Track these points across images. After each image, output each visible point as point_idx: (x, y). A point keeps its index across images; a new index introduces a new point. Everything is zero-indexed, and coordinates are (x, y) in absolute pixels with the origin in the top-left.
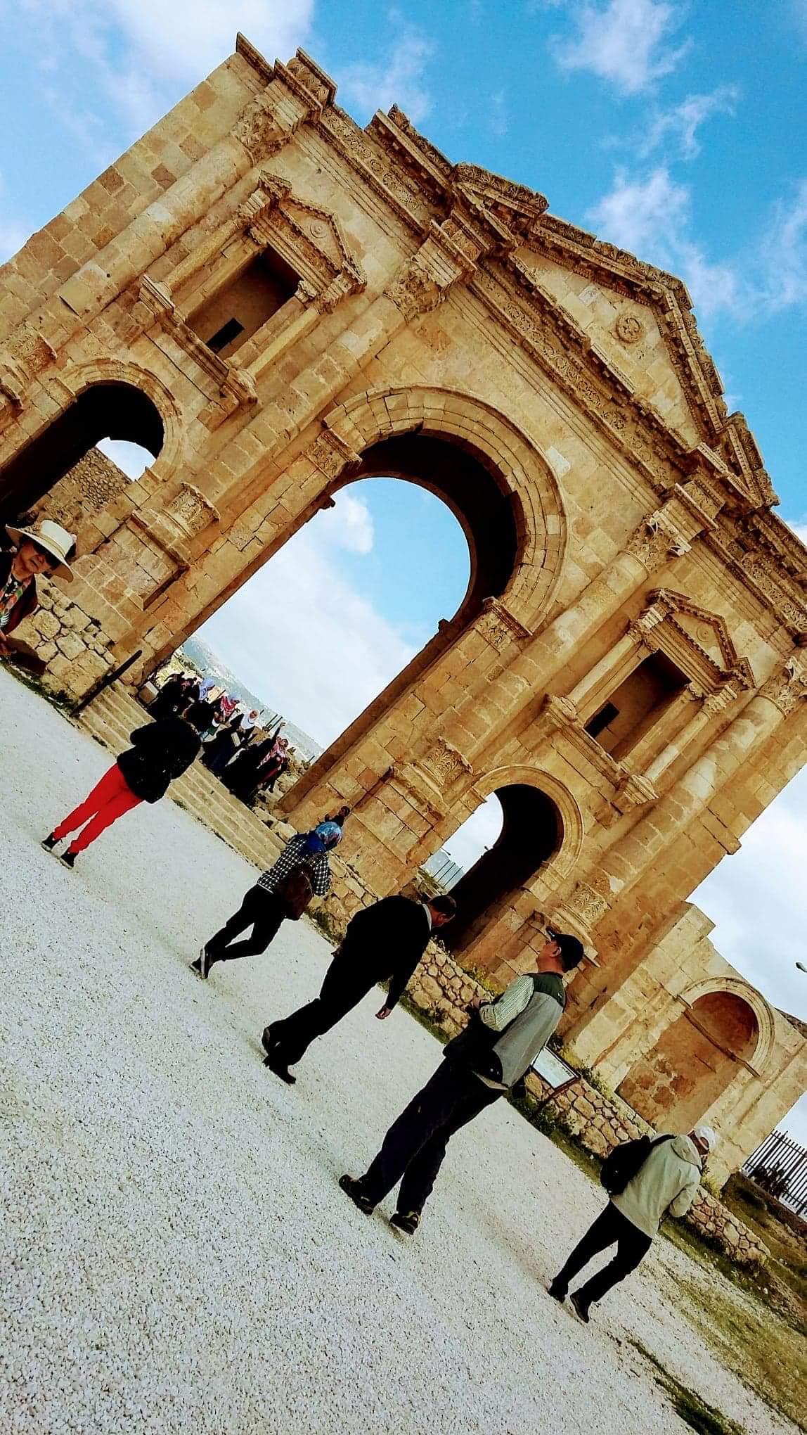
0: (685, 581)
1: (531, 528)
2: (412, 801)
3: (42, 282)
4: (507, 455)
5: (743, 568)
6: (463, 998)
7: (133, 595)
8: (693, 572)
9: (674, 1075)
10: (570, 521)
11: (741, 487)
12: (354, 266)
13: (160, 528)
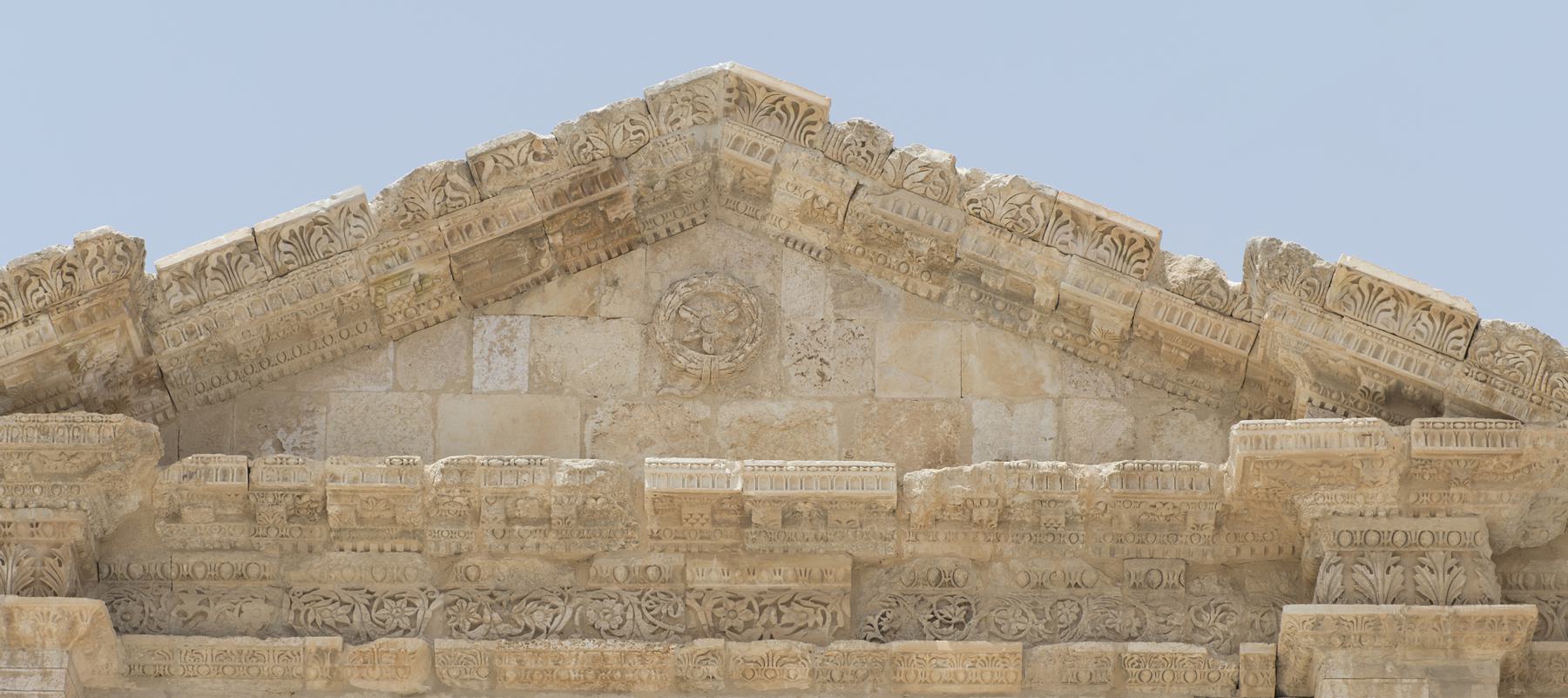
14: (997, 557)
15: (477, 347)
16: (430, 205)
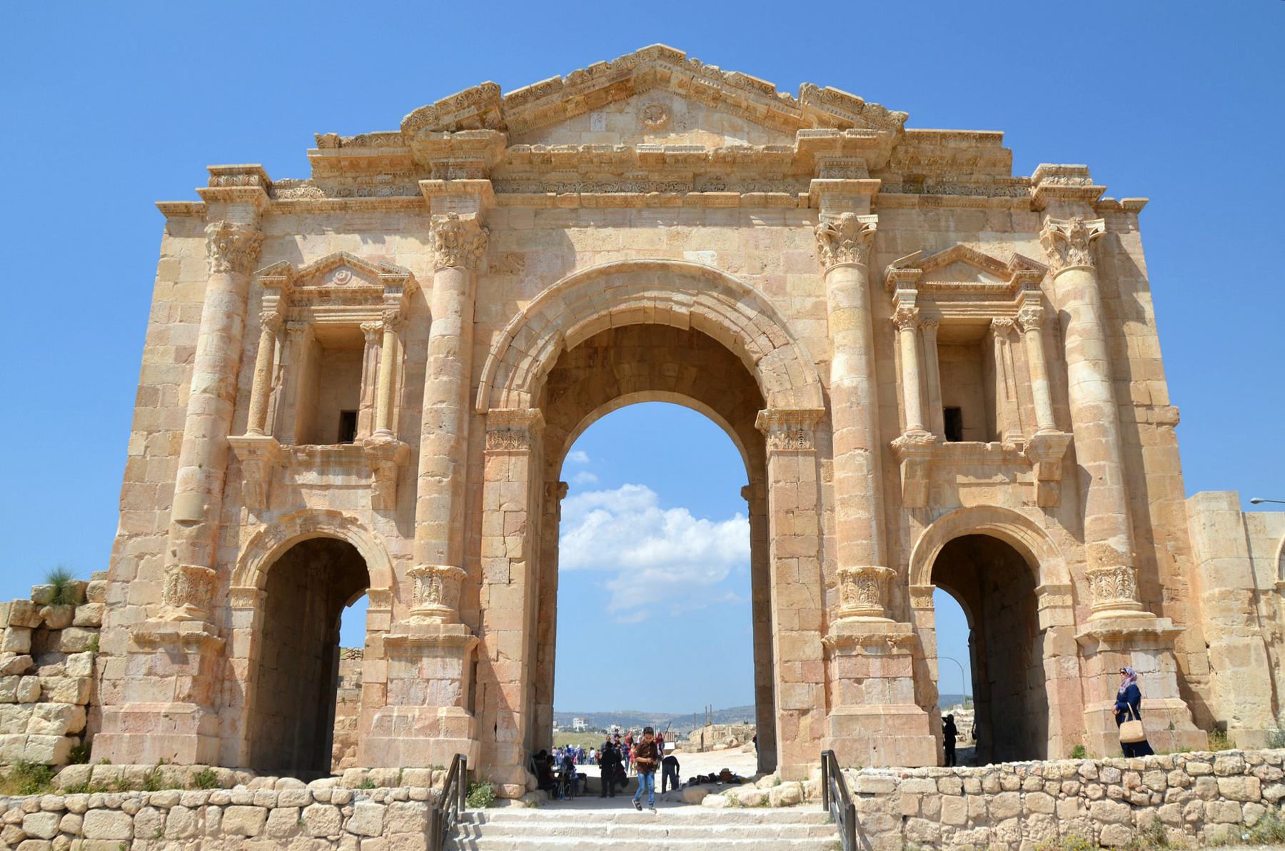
0: (899, 248)
1: (734, 328)
3: (156, 525)
5: (932, 195)
6: (1156, 787)
7: (449, 711)
8: (899, 236)
10: (759, 290)
11: (865, 134)
12: (390, 272)
13: (419, 628)
14: (732, 172)
15: (592, 120)
16: (579, 81)
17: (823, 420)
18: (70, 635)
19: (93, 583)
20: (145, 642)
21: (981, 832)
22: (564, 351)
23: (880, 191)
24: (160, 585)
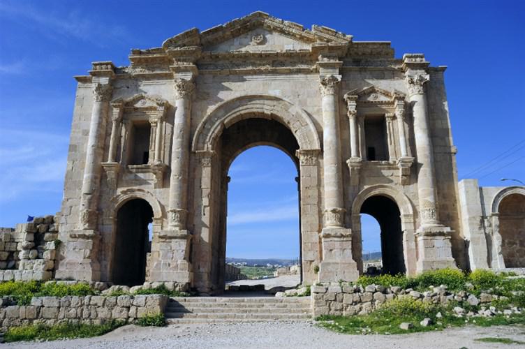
2: (336, 239)
4: (258, 106)
9: (518, 242)
17: (320, 153)
18: (47, 235)
19: (56, 216)
20: (73, 237)
21: (357, 307)
22: (225, 128)
23: (343, 65)
24: (78, 216)
